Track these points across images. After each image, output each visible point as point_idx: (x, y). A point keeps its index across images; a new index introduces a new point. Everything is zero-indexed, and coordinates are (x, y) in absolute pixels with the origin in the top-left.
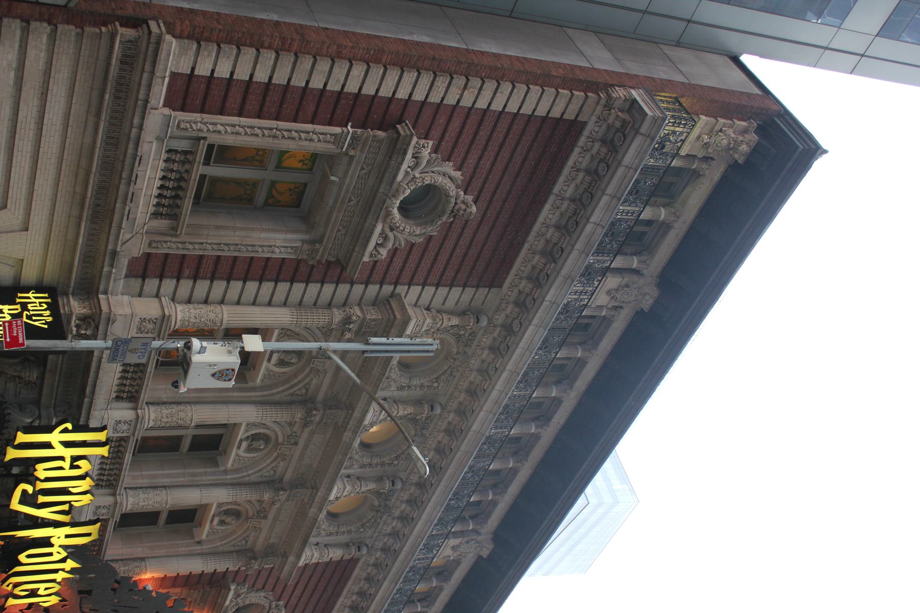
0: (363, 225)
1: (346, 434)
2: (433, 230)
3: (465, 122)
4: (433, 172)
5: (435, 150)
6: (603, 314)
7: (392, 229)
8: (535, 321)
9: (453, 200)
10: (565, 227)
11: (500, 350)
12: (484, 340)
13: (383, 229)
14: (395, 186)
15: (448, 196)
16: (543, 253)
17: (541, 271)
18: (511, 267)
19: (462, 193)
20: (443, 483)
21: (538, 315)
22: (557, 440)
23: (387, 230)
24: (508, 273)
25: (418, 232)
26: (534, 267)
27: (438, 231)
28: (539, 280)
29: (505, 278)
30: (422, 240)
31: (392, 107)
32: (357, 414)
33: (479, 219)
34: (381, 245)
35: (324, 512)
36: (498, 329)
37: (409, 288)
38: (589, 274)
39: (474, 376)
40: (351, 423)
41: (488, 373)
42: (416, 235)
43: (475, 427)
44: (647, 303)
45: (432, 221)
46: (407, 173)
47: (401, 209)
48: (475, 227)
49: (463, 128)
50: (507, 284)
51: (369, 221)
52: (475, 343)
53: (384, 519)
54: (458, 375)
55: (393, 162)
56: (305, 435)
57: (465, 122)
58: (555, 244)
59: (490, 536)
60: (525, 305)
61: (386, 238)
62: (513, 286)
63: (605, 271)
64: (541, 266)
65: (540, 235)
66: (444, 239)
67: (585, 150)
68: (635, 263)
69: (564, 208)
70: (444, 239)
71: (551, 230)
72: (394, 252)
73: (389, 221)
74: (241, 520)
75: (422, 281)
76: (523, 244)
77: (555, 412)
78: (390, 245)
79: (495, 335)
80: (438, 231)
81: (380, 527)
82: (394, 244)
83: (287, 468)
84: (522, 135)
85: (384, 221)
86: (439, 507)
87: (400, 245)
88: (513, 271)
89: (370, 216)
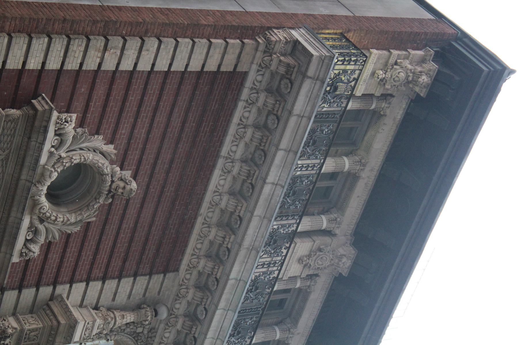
0: (7, 221)
2: (90, 215)
3: (110, 89)
4: (81, 149)
5: (81, 124)
6: (298, 286)
7: (42, 221)
8: (222, 304)
9: (109, 179)
10: (240, 192)
12: (167, 335)
13: (31, 223)
14: (39, 170)
15: (102, 174)
16: (219, 225)
17: (220, 245)
18: (186, 246)
19: (118, 169)
21: (224, 297)
23: (37, 223)
24: (183, 253)
25: (73, 220)
26: (211, 243)
27: (96, 216)
28: (220, 256)
29: (181, 260)
30: (78, 228)
31: (24, 80)
33: (142, 196)
34: (31, 241)
36: (181, 321)
37: (71, 287)
38: (275, 242)
42: (71, 224)
44: (345, 265)
45: (88, 206)
46: (51, 154)
47: (51, 196)
48: (138, 206)
49: (108, 95)
50: (183, 266)
51: (13, 214)
52: (157, 340)
55: (33, 143)
57: (110, 89)
58: (232, 213)
60: (208, 287)
61: (36, 232)
62: (191, 267)
63: (292, 236)
64: (219, 240)
65: (214, 205)
66: (105, 224)
67: (250, 103)
68: (324, 222)
69: (235, 171)
70: (105, 224)
71: (225, 198)
72: (48, 246)
73: (37, 212)
75: (85, 277)
76: (196, 218)
78: (42, 239)
79: (179, 326)
80: (96, 216)
82: (47, 238)
84: (177, 95)
85: (32, 213)
87: (54, 238)
88: (189, 250)
89: (15, 209)
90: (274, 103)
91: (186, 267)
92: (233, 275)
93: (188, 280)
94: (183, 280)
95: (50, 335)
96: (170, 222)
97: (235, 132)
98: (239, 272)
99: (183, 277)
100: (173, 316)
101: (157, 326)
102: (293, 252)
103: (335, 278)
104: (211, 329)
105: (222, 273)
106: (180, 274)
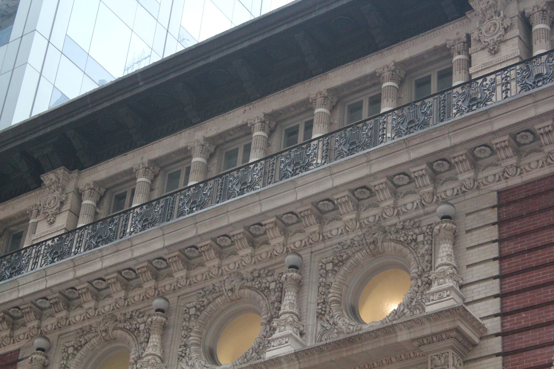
8: (14, 296)
11: (68, 298)
20: (257, 210)
22: (245, 100)
39: (277, 240)
41: (97, 287)
43: (158, 245)
52: (87, 323)
53: (395, 220)
54: (131, 309)
59: (469, 14)
77: (233, 129)
79: (64, 314)
81: (415, 214)
86: (300, 182)
91: (17, 343)
93: (24, 334)
94: (27, 338)
100: (211, 275)
101: (74, 333)
102: (40, 237)
103: (80, 170)
104: (37, 290)
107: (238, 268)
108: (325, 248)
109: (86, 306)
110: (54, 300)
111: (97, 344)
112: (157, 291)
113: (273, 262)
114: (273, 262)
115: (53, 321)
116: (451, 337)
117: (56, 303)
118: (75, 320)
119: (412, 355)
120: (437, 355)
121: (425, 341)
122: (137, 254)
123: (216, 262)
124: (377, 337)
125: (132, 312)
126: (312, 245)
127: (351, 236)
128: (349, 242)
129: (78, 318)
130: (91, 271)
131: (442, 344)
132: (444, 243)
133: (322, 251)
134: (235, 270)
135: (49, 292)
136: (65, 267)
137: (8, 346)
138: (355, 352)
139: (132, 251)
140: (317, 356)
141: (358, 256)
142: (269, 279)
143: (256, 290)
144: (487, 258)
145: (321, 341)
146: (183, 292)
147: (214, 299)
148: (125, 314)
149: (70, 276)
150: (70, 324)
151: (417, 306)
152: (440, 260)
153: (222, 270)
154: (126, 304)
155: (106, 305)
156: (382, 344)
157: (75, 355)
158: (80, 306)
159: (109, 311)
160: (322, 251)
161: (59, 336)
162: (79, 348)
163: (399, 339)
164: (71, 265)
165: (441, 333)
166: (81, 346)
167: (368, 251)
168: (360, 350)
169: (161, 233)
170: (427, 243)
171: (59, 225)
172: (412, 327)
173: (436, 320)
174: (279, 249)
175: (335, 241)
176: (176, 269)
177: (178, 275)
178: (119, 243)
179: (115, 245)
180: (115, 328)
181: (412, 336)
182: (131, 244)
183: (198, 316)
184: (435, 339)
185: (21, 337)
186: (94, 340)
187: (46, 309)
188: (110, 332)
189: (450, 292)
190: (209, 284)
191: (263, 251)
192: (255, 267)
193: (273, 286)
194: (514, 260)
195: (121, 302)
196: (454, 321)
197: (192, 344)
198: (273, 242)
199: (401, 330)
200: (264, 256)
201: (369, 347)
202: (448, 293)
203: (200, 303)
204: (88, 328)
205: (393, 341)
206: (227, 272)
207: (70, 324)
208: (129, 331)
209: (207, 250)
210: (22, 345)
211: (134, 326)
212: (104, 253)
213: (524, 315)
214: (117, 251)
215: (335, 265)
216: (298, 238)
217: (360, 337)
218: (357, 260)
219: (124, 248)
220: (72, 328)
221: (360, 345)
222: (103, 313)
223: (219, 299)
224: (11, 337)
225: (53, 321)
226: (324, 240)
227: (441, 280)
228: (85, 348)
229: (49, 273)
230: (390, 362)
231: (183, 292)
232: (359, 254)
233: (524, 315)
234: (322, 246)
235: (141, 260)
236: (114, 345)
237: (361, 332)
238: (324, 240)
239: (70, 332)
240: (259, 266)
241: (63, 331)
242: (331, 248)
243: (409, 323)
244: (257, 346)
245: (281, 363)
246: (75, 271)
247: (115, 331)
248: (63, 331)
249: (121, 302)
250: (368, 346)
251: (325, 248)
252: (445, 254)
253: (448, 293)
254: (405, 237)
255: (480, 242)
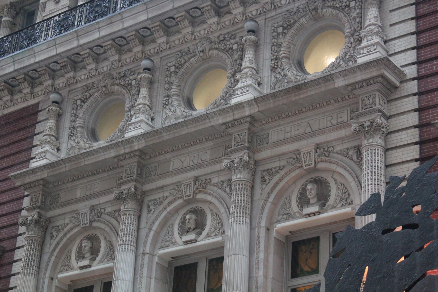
1: (136, 148)
8: (32, 61)
11: (74, 61)
18: (24, 109)
21: (26, 64)
24: (29, 107)
32: (45, 174)
35: (96, 145)
40: (122, 152)
41: (97, 52)
43: (143, 17)
52: (90, 81)
56: (168, 181)
74: (199, 205)
76: (6, 115)
79: (72, 74)
83: (218, 172)
90: (86, 59)
92: (11, 69)
93: (42, 91)
94: (44, 94)
95: (30, 187)
96: (4, 133)
97: (32, 100)
98: (9, 66)
99: (42, 96)
100: (186, 40)
101: (81, 88)
102: (49, 14)
105: (19, 76)
106: (42, 98)
107: (207, 33)
108: (276, 15)
109: (89, 67)
110: (63, 64)
111: (99, 97)
112: (144, 54)
113: (235, 28)
114: (235, 28)
115: (64, 80)
116: (378, 82)
117: (65, 66)
118: (81, 79)
119: (347, 97)
120: (366, 97)
121: (357, 86)
122: (126, 25)
123: (190, 29)
124: (319, 84)
125: (125, 71)
126: (266, 13)
127: (297, 5)
128: (295, 10)
129: (83, 77)
130: (91, 40)
131: (370, 88)
132: (371, 8)
133: (274, 18)
134: (205, 35)
135: (58, 57)
136: (70, 37)
137: (30, 100)
138: (302, 96)
139: (123, 23)
140: (272, 101)
141: (303, 20)
142: (232, 41)
143: (222, 50)
144: (406, 18)
145: (274, 89)
146: (164, 54)
147: (189, 59)
148: (120, 73)
149: (75, 44)
150: (77, 82)
151: (350, 59)
152: (368, 21)
153: (195, 36)
154: (120, 66)
155: (105, 67)
156: (323, 89)
157: (83, 106)
158: (84, 68)
159: (107, 71)
160: (274, 18)
161: (69, 91)
162: (85, 100)
163: (336, 85)
164: (75, 35)
165: (369, 79)
166: (87, 99)
167: (311, 16)
168: (306, 95)
169: (145, 7)
170: (358, 8)
171: (63, 4)
172: (347, 75)
173: (365, 69)
174: (239, 17)
175: (284, 9)
176: (158, 36)
177: (160, 41)
178: (112, 17)
179: (108, 18)
180: (113, 84)
181: (347, 82)
182: (122, 17)
183: (177, 73)
184: (364, 84)
185: (40, 93)
186: (97, 94)
187: (57, 70)
188: (109, 87)
189: (377, 47)
190: (184, 47)
191: (226, 19)
192: (220, 32)
193: (235, 47)
194: (427, 19)
195: (116, 64)
196: (380, 69)
197: (173, 95)
198: (234, 12)
199: (338, 78)
200: (227, 23)
201: (313, 93)
202: (375, 47)
203: (179, 62)
204: (91, 85)
205: (332, 87)
206: (198, 37)
207: (77, 82)
208: (124, 86)
209: (182, 20)
210: (41, 99)
211: (127, 82)
212: (101, 25)
213: (435, 63)
214: (111, 23)
215: (284, 28)
216: (255, 8)
217: (305, 84)
218: (302, 24)
219: (116, 20)
220: (79, 85)
221: (305, 91)
222: (102, 73)
223: (193, 59)
224: (31, 93)
225: (64, 80)
226: (275, 8)
227: (370, 37)
228: (89, 101)
229: (58, 42)
230: (329, 103)
231: (164, 54)
232: (304, 19)
233: (435, 63)
234: (274, 13)
235: (130, 29)
236: (112, 97)
237: (306, 81)
238: (275, 8)
239: (77, 88)
240: (224, 32)
241: (72, 88)
242: (281, 15)
243: (344, 72)
244: (224, 95)
245: (243, 107)
246: (78, 40)
247: (113, 87)
248: (72, 88)
249: (116, 64)
250: (312, 92)
251: (276, 15)
252: (372, 16)
253: (375, 47)
254: (340, 4)
255: (401, 6)
